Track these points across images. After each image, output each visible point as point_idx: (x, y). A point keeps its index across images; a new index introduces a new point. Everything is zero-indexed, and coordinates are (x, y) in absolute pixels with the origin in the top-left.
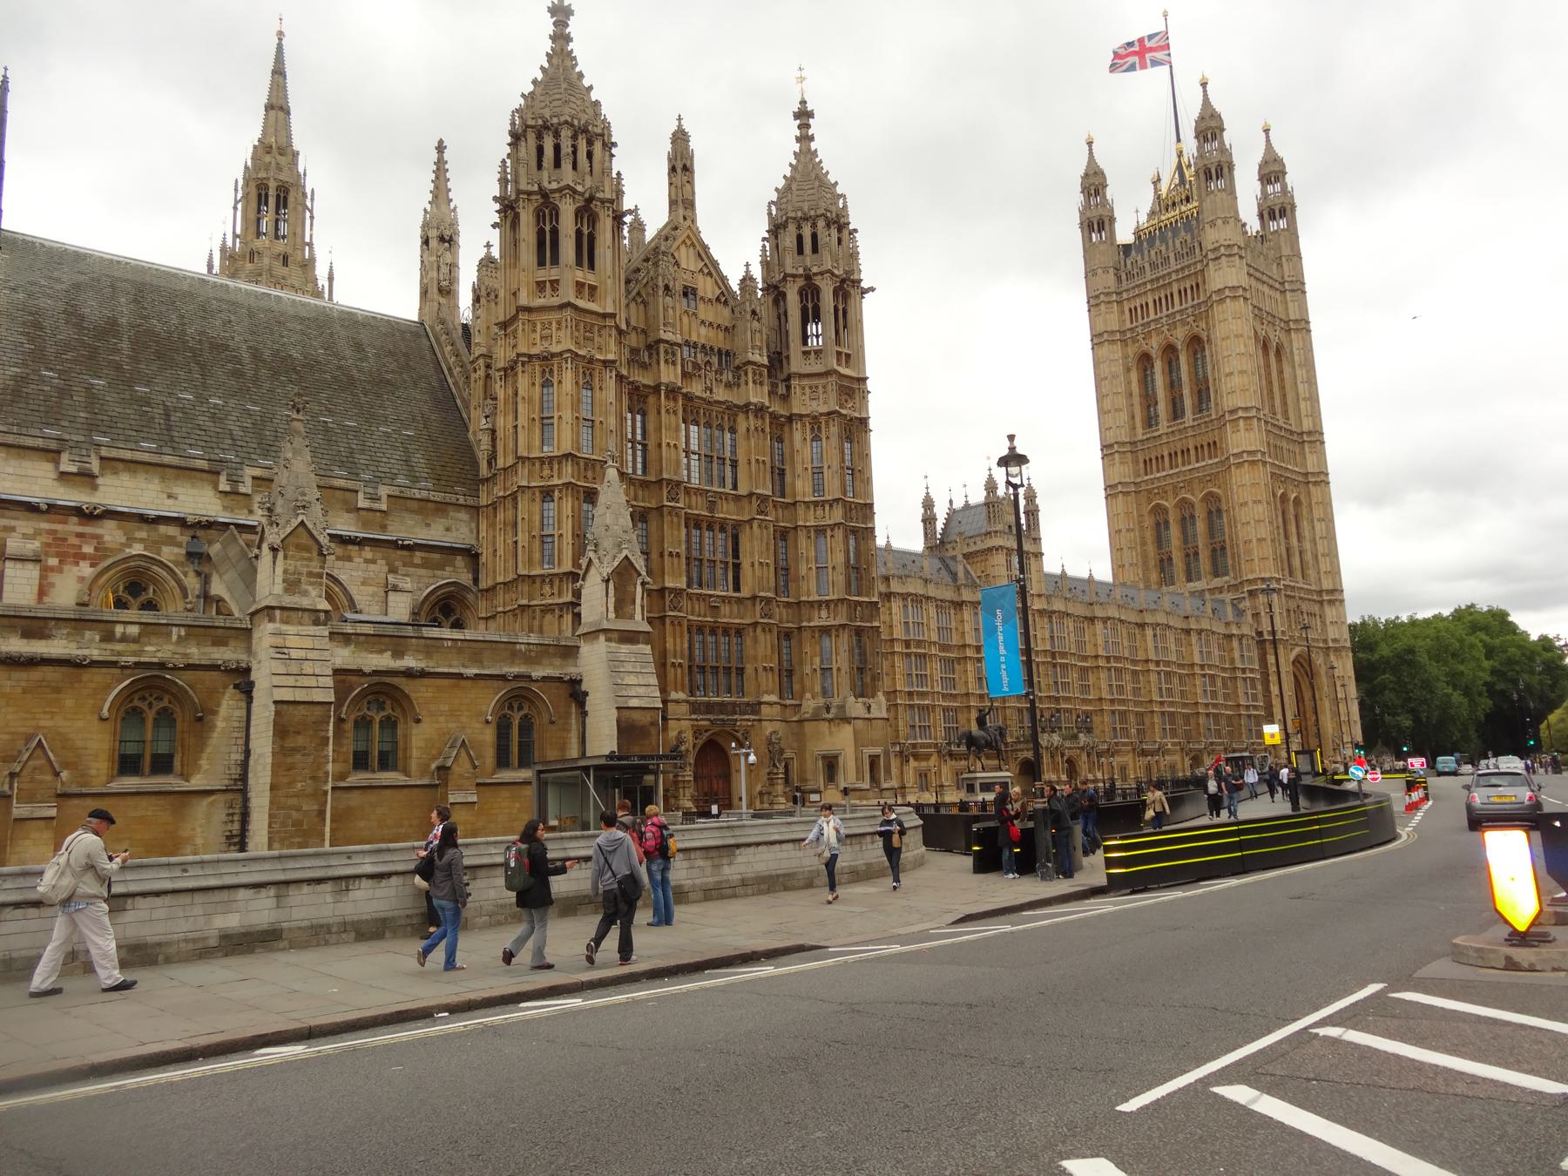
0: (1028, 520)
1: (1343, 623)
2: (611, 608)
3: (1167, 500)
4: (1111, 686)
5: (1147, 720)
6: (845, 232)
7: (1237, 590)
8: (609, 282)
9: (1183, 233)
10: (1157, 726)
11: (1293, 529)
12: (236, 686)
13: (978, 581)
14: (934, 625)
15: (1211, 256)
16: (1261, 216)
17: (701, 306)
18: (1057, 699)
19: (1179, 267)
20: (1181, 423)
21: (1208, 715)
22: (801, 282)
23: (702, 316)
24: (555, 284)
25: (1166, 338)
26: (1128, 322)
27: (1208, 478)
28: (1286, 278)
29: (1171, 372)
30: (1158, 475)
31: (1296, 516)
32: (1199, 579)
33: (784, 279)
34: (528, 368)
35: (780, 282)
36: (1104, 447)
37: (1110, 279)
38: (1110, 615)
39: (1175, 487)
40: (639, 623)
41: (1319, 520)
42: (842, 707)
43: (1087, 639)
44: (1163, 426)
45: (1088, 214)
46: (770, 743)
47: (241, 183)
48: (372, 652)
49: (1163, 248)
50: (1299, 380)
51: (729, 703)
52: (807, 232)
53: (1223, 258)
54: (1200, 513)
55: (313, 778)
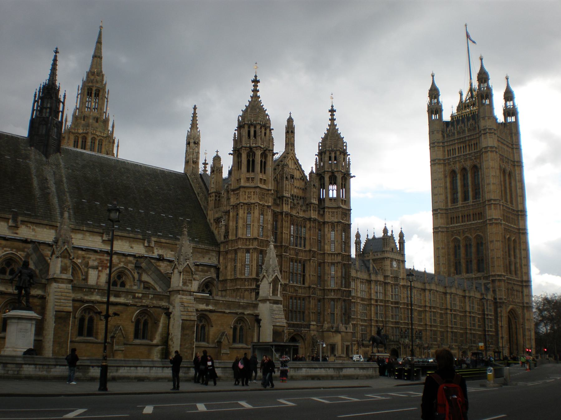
2: (271, 292)
3: (460, 236)
4: (431, 319)
5: (445, 335)
6: (346, 155)
8: (270, 178)
9: (471, 121)
10: (449, 338)
11: (512, 253)
12: (165, 313)
13: (378, 271)
15: (482, 132)
16: (504, 114)
17: (295, 181)
19: (469, 134)
20: (468, 203)
22: (330, 174)
23: (295, 185)
24: (253, 179)
25: (463, 165)
26: (447, 156)
28: (514, 143)
30: (457, 225)
32: (471, 273)
33: (324, 172)
34: (243, 207)
35: (322, 173)
37: (439, 136)
38: (432, 288)
40: (279, 297)
42: (338, 327)
44: (460, 203)
46: (313, 339)
47: (81, 87)
48: (200, 304)
50: (518, 188)
51: (300, 324)
52: (333, 155)
53: (488, 133)
54: (473, 243)
55: (191, 343)
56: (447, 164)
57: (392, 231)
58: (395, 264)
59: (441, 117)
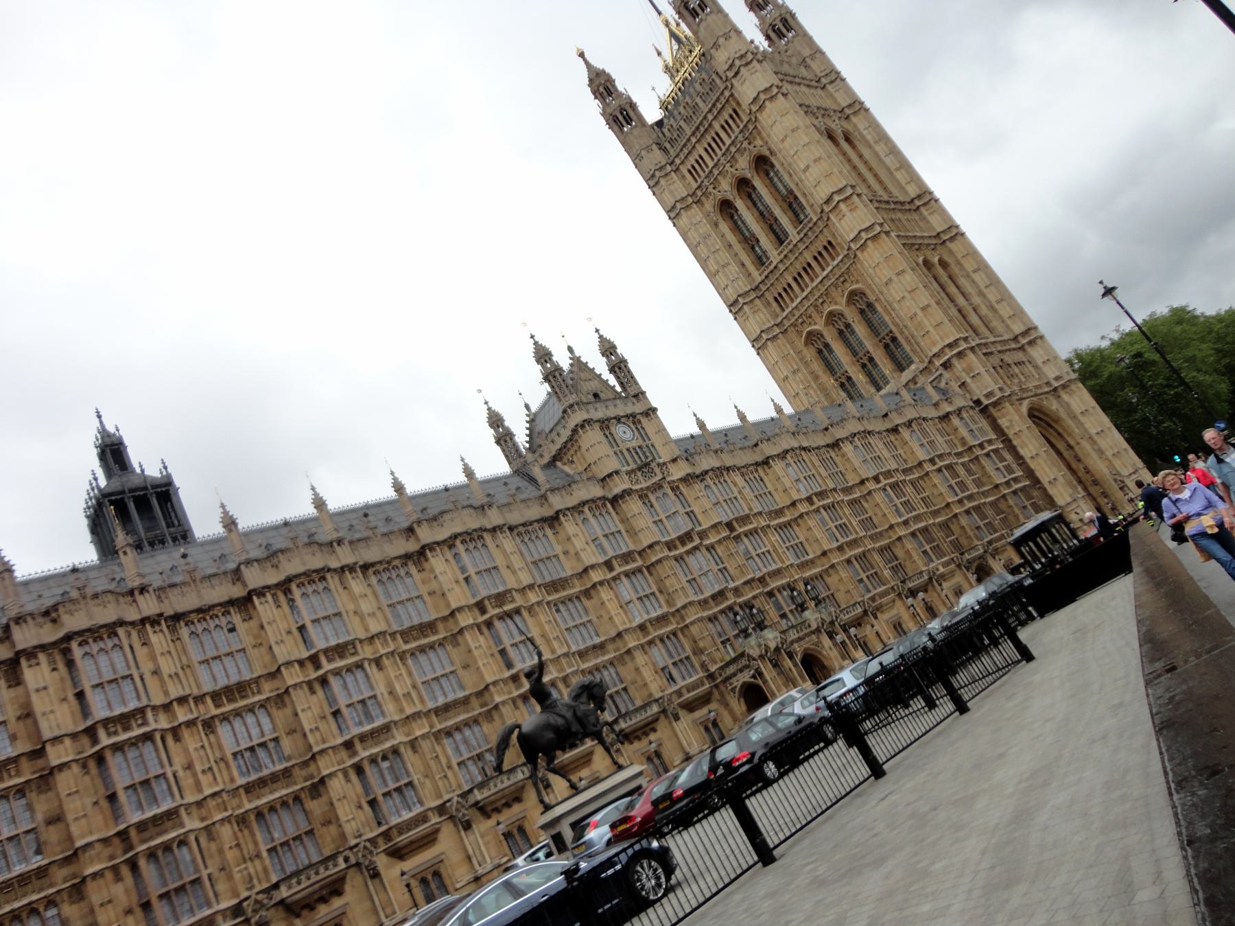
0: (618, 378)
1: (1056, 357)
3: (815, 324)
5: (899, 552)
7: (931, 373)
10: (914, 554)
11: (952, 289)
14: (517, 562)
15: (730, 74)
16: (768, 37)
18: (762, 580)
19: (710, 106)
21: (968, 512)
27: (842, 279)
28: (820, 75)
29: (755, 204)
30: (794, 305)
31: (951, 277)
37: (657, 156)
39: (816, 306)
41: (975, 271)
43: (770, 488)
44: (774, 256)
45: (609, 111)
49: (688, 99)
50: (882, 156)
54: (852, 316)
56: (703, 199)
57: (570, 349)
58: (623, 432)
59: (640, 118)
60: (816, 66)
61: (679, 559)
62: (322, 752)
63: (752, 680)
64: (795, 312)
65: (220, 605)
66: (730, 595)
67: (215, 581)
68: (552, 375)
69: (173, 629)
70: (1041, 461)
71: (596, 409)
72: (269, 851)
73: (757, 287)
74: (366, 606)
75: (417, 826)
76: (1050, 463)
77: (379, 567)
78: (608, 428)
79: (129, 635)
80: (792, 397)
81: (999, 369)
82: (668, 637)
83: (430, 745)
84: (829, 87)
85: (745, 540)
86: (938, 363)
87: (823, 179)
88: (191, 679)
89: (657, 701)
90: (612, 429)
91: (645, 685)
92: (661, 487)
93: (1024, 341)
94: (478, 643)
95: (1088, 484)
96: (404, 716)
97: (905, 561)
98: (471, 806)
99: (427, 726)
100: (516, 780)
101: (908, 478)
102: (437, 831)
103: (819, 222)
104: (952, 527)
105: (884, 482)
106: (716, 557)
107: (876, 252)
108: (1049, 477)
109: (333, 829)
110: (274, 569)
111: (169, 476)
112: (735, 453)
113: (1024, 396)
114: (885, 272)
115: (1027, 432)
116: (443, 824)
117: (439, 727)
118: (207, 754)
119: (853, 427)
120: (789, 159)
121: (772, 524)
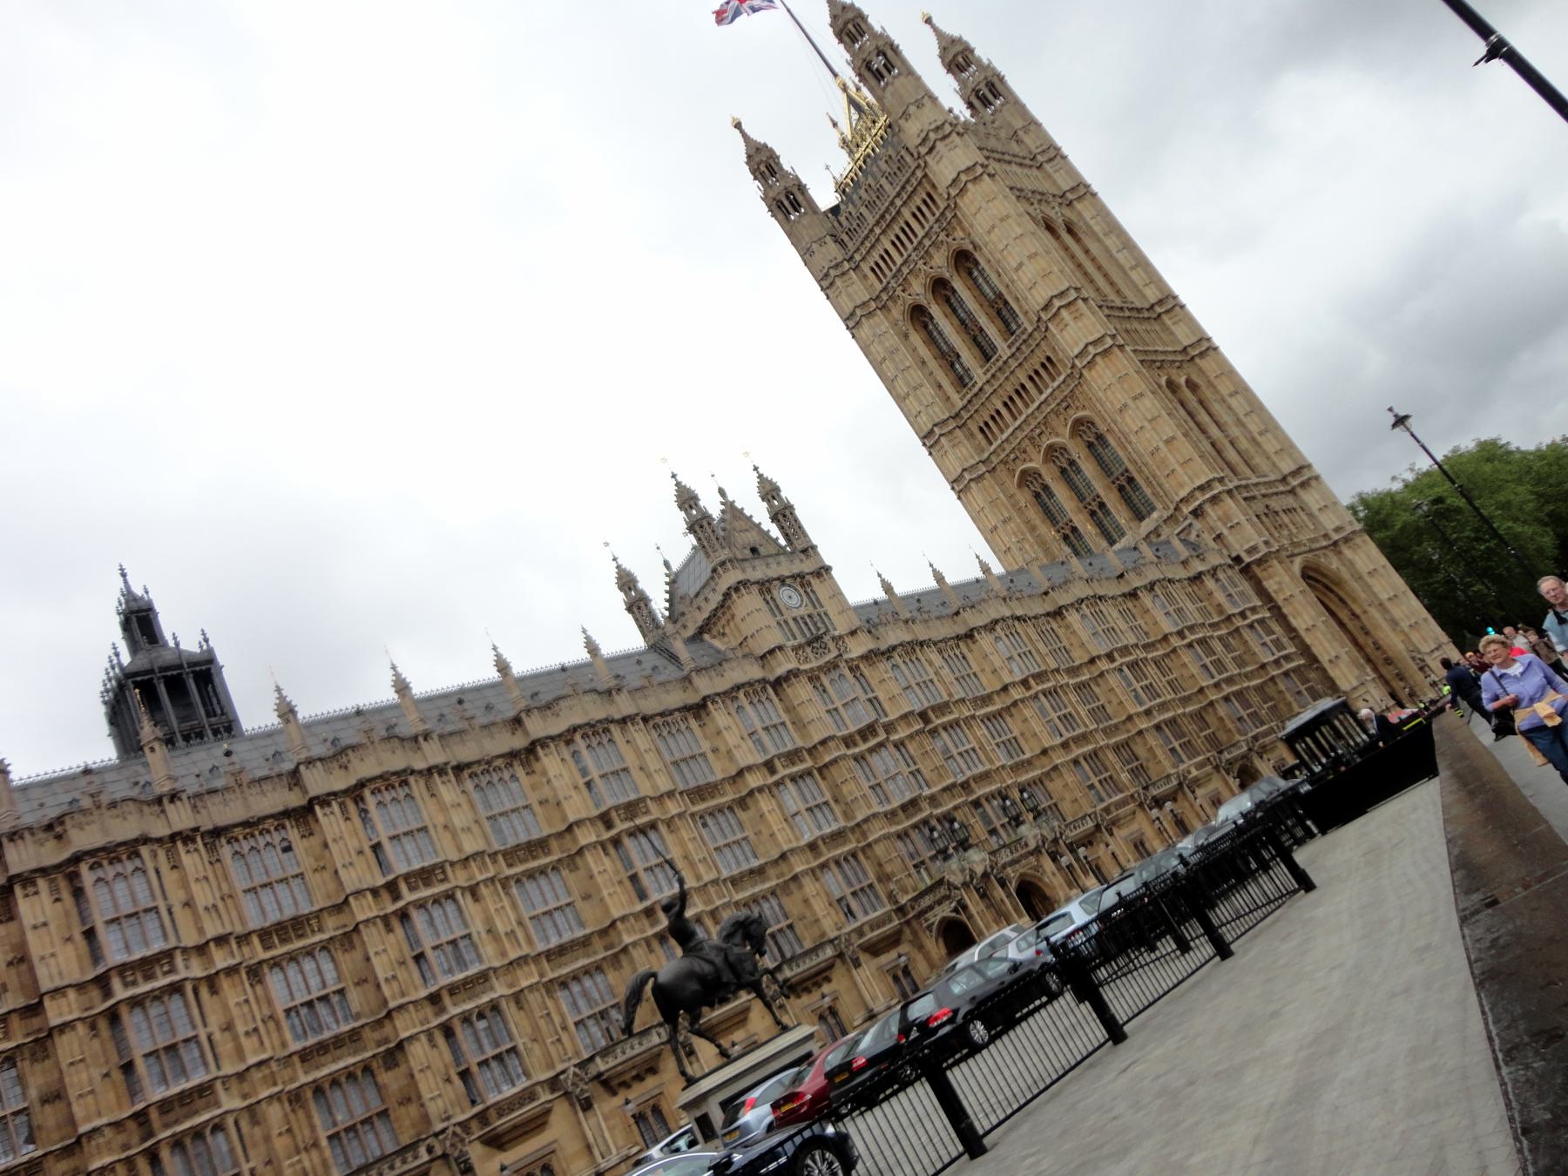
0: (781, 528)
1: (1335, 503)
3: (1031, 460)
5: (1140, 750)
7: (1177, 522)
10: (1159, 752)
11: (1203, 417)
14: (653, 763)
15: (923, 150)
16: (970, 105)
18: (965, 786)
19: (898, 189)
21: (1226, 699)
27: (1064, 404)
29: (954, 311)
30: (1005, 436)
31: (1201, 402)
36: (924, 438)
37: (833, 250)
38: (995, 615)
39: (1031, 439)
41: (1231, 395)
43: (976, 668)
44: (979, 375)
45: (771, 194)
49: (871, 181)
50: (1114, 252)
53: (938, 143)
54: (1077, 451)
56: (890, 304)
57: (722, 492)
58: (788, 597)
59: (811, 203)
60: (1029, 140)
61: (858, 758)
62: (401, 1007)
63: (954, 914)
64: (1005, 445)
65: (272, 816)
66: (925, 805)
67: (267, 786)
68: (699, 525)
69: (211, 848)
70: (1319, 635)
71: (754, 568)
72: (330, 1138)
73: (957, 415)
74: (459, 819)
75: (522, 1105)
76: (1329, 636)
77: (477, 769)
78: (769, 591)
79: (155, 855)
80: (1002, 553)
81: (1264, 518)
82: (846, 859)
83: (539, 1000)
84: (1047, 167)
85: (944, 734)
86: (1186, 509)
87: (1040, 281)
88: (234, 914)
89: (831, 941)
90: (775, 592)
91: (817, 921)
92: (836, 667)
93: (1295, 482)
94: (601, 866)
95: (1380, 662)
96: (507, 961)
97: (1148, 761)
98: (592, 1080)
99: (536, 974)
100: (650, 1045)
101: (1150, 656)
102: (548, 1112)
103: (1036, 333)
104: (1207, 718)
105: (1119, 661)
106: (907, 756)
107: (1108, 372)
108: (1328, 652)
109: (413, 1109)
110: (343, 771)
111: (210, 651)
112: (931, 624)
113: (1296, 551)
114: (1119, 396)
115: (1300, 597)
116: (556, 1102)
117: (551, 975)
118: (251, 1011)
119: (1080, 590)
120: (998, 256)
121: (977, 713)
